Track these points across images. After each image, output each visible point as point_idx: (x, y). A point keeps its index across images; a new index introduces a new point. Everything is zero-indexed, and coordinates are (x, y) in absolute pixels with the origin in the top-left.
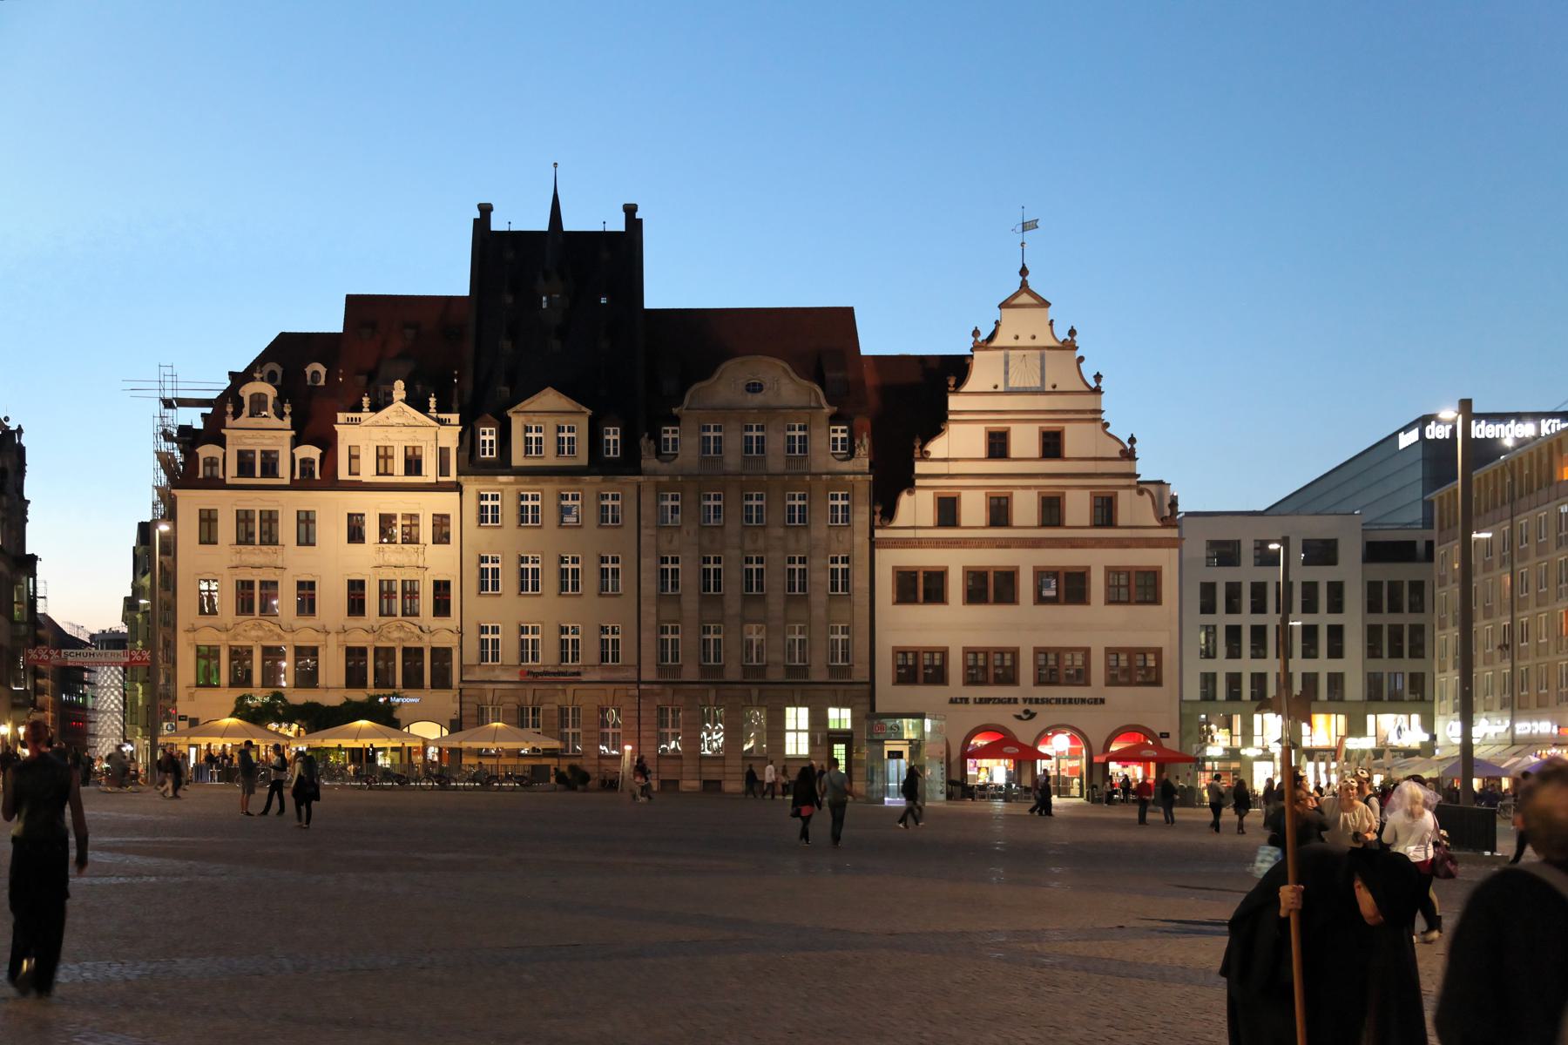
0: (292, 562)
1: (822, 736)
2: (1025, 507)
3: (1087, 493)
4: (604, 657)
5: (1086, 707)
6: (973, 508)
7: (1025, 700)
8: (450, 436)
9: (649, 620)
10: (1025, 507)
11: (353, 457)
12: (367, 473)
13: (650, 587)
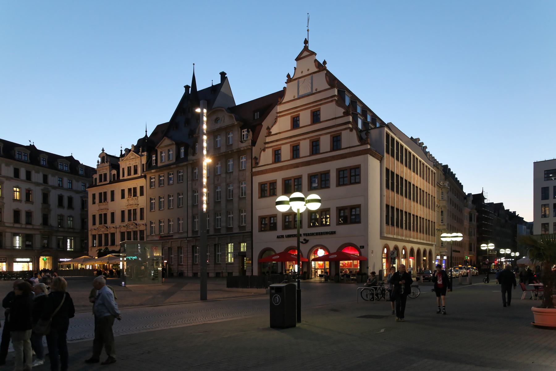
1: (239, 255)
3: (329, 136)
5: (329, 236)
7: (304, 234)
8: (144, 160)
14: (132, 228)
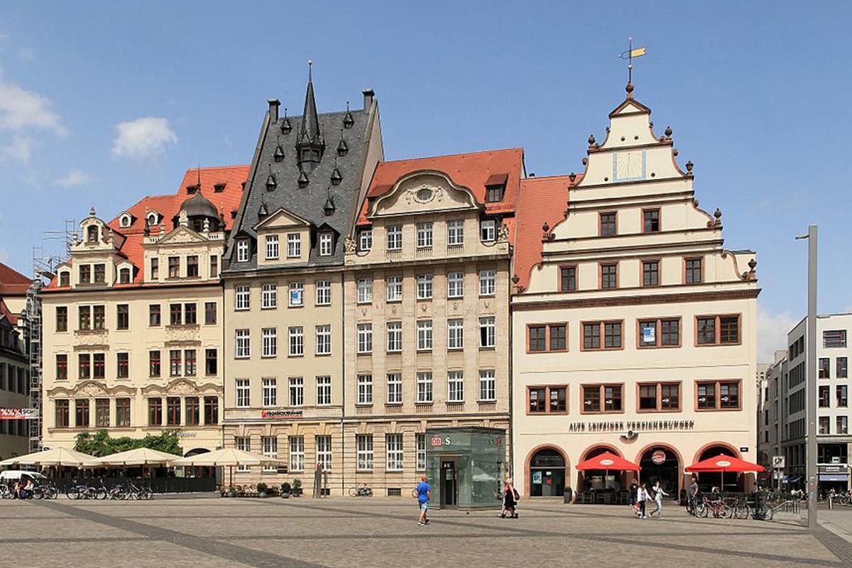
0: (114, 341)
2: (630, 273)
3: (680, 259)
4: (320, 400)
6: (589, 276)
8: (218, 251)
9: (351, 373)
10: (630, 273)
11: (154, 268)
12: (163, 275)
13: (352, 347)
14: (182, 391)
